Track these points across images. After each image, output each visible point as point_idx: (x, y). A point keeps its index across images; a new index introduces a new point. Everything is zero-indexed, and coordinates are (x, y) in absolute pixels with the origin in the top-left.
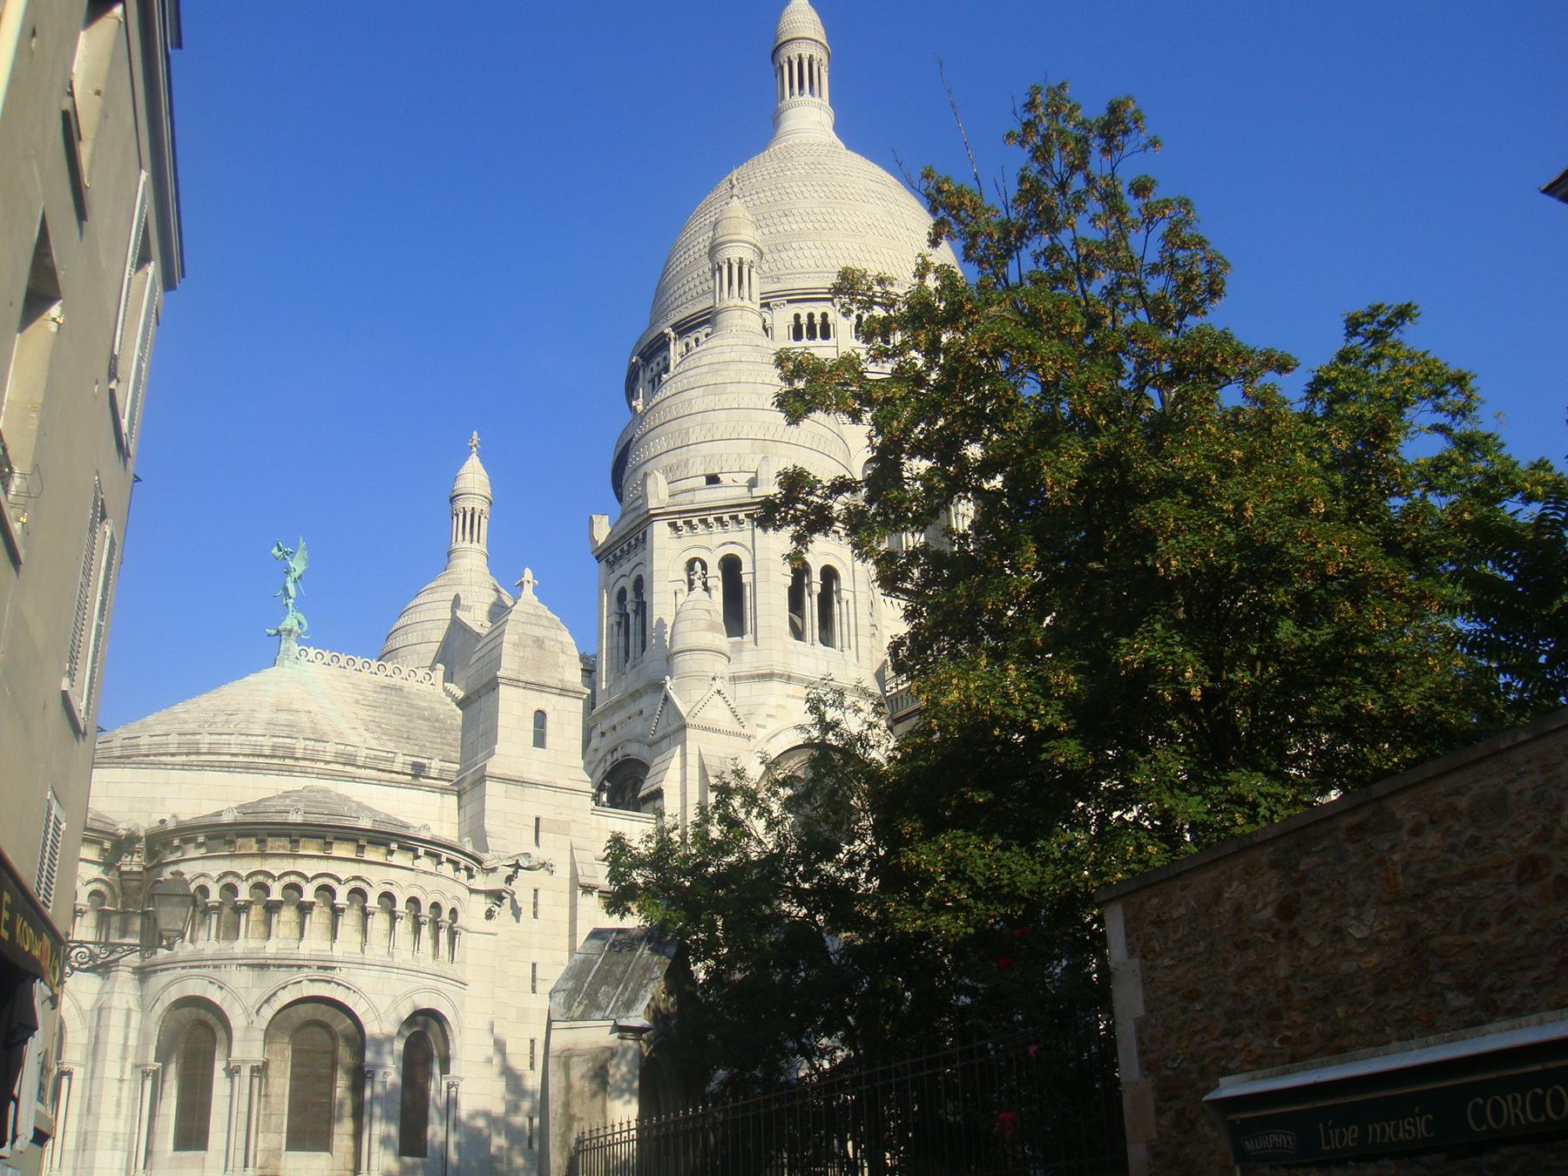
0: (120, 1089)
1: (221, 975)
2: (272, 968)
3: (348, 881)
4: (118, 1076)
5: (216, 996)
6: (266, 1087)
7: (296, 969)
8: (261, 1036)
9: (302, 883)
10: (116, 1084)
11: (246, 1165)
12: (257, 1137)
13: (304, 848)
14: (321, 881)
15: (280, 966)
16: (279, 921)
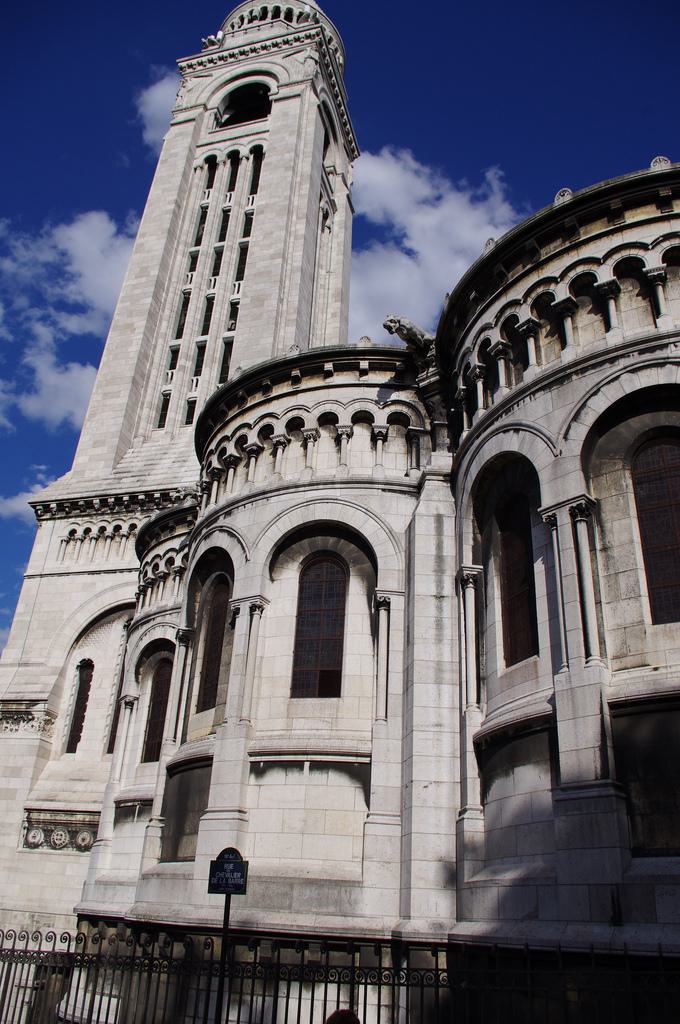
0: (440, 609)
1: (518, 414)
2: (574, 377)
3: (656, 243)
4: (433, 591)
5: (512, 443)
6: (603, 538)
7: (607, 365)
8: (574, 465)
9: (594, 268)
10: (433, 601)
11: (588, 654)
12: (599, 610)
13: (586, 233)
14: (617, 257)
15: (584, 370)
16: (575, 328)
